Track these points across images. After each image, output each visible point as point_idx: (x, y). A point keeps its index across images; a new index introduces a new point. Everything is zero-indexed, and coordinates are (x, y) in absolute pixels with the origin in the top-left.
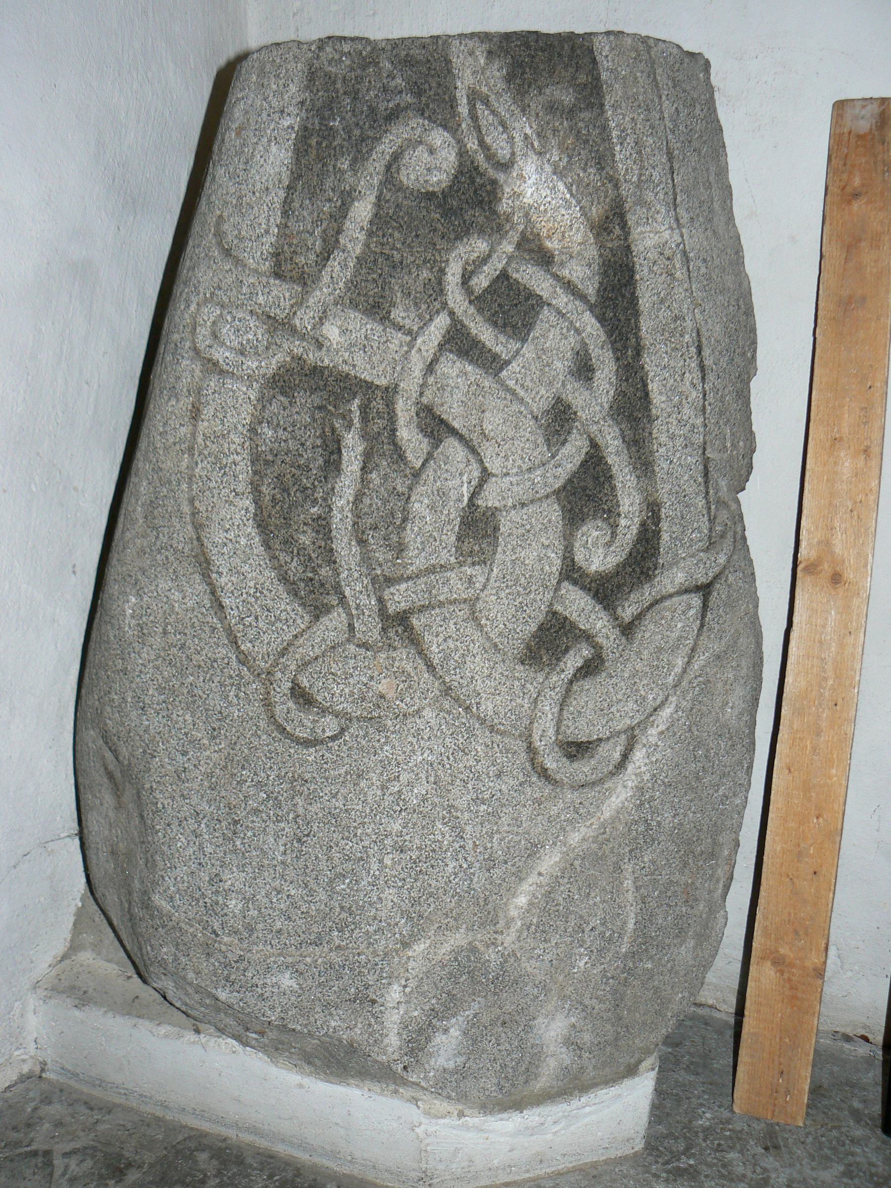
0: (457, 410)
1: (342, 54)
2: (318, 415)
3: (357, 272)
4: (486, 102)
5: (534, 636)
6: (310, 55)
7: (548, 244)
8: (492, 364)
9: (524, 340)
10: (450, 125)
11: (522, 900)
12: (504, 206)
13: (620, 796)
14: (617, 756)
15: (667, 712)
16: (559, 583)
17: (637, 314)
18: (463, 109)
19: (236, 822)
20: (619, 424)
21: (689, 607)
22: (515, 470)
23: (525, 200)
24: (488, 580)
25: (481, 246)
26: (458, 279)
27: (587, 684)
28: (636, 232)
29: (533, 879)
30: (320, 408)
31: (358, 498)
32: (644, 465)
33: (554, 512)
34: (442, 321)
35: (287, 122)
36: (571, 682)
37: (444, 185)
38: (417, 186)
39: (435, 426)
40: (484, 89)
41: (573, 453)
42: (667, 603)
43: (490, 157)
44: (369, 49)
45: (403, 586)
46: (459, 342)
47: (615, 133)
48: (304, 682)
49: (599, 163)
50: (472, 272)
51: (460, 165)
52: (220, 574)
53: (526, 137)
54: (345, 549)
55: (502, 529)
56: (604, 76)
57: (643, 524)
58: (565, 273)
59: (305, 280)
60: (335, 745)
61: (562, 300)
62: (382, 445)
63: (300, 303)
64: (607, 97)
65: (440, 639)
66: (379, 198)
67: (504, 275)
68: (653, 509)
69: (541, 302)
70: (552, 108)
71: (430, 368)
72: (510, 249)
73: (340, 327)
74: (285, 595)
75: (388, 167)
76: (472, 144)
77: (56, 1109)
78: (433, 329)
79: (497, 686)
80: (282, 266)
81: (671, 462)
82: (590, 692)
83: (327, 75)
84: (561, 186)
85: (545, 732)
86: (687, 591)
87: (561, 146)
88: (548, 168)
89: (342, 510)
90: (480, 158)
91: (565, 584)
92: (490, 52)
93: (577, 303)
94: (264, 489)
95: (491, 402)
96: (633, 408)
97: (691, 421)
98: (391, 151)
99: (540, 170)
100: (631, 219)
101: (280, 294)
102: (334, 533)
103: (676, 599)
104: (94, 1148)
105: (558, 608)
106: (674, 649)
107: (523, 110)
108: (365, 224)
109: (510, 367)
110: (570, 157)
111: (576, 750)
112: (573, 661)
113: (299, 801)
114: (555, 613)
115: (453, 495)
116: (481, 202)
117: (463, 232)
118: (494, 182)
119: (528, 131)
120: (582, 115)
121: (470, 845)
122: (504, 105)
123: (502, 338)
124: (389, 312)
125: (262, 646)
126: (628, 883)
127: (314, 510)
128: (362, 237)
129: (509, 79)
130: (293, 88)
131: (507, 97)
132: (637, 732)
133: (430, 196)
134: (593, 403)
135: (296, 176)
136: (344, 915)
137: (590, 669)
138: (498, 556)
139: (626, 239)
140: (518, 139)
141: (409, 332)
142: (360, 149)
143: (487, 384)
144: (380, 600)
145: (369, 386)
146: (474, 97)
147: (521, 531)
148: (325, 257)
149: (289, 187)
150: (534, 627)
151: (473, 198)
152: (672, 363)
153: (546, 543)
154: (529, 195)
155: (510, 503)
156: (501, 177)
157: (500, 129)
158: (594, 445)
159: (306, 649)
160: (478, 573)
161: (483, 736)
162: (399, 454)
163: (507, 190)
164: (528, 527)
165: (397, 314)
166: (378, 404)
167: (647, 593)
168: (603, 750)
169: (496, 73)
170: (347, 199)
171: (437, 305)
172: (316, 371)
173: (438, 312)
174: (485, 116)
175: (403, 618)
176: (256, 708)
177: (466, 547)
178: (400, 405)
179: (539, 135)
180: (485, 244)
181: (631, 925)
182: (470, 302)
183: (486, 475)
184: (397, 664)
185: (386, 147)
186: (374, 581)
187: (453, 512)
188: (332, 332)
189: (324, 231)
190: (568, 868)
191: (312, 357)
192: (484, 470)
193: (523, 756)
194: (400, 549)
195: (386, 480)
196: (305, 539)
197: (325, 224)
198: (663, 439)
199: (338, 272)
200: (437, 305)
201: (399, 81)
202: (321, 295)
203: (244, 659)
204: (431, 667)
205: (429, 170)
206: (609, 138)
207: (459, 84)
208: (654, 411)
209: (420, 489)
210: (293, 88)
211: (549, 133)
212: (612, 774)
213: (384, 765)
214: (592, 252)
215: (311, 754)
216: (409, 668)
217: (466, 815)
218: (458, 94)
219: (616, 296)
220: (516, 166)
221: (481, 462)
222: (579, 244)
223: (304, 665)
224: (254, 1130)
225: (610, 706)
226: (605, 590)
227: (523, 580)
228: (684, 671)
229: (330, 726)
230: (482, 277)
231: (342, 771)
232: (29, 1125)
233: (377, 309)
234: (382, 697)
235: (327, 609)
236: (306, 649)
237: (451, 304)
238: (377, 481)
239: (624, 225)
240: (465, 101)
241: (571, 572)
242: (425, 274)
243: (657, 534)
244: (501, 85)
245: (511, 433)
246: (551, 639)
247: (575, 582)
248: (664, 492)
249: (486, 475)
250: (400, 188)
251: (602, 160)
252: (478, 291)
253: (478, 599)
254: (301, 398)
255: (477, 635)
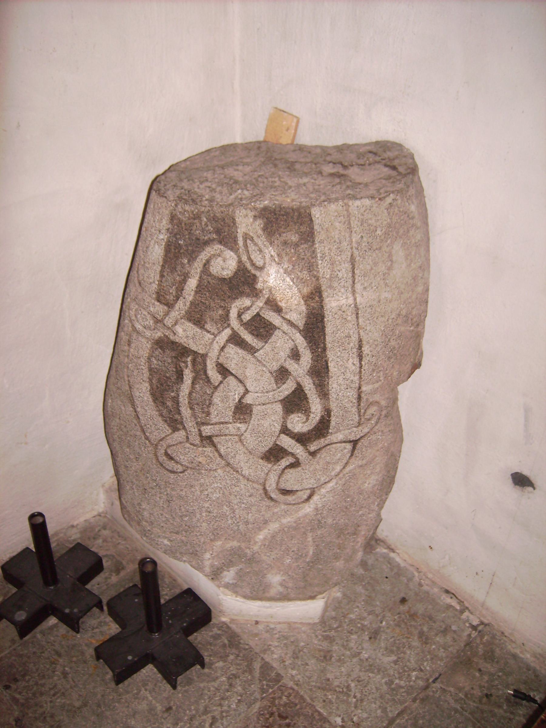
0: (233, 366)
1: (185, 211)
2: (174, 360)
3: (190, 308)
4: (252, 239)
5: (267, 451)
6: (172, 208)
7: (280, 304)
8: (252, 350)
9: (266, 342)
10: (234, 248)
11: (261, 537)
12: (259, 286)
13: (308, 509)
14: (305, 497)
15: (331, 485)
16: (279, 434)
17: (324, 335)
18: (241, 242)
19: (145, 489)
20: (312, 378)
21: (345, 448)
22: (260, 392)
23: (269, 284)
24: (247, 429)
25: (247, 302)
26: (236, 315)
27: (291, 471)
28: (326, 300)
29: (266, 531)
30: (175, 357)
31: (190, 393)
32: (324, 394)
33: (279, 408)
34: (227, 332)
35: (161, 237)
36: (284, 469)
37: (230, 276)
38: (217, 275)
39: (224, 371)
40: (251, 234)
41: (288, 388)
42: (334, 446)
43: (253, 264)
44: (196, 211)
45: (209, 427)
46: (236, 340)
47: (319, 255)
48: (169, 452)
49: (309, 269)
50: (243, 313)
51: (239, 266)
52: (138, 407)
53: (272, 256)
54: (186, 412)
55: (254, 412)
56: (316, 227)
57: (322, 416)
58: (288, 317)
59: (170, 306)
60: (181, 475)
61: (286, 327)
62: (200, 374)
63: (167, 314)
64: (317, 238)
65: (225, 447)
66: (200, 277)
67: (258, 315)
68: (328, 412)
69: (275, 328)
70: (285, 243)
71: (223, 349)
72: (261, 305)
73: (183, 329)
74: (161, 421)
75: (205, 265)
76: (244, 258)
77: (106, 533)
78: (223, 334)
79: (252, 467)
80: (160, 297)
81: (338, 395)
82: (291, 474)
83: (179, 219)
84: (288, 279)
85: (271, 485)
86: (344, 442)
87: (290, 261)
88: (282, 271)
89: (183, 396)
90: (248, 265)
91: (283, 436)
92: (255, 216)
93: (293, 329)
94: (153, 381)
95: (250, 366)
96: (320, 372)
97: (351, 379)
98: (206, 259)
99: (277, 272)
100: (325, 295)
101: (159, 309)
102: (180, 404)
103: (339, 445)
104: (113, 556)
105: (278, 443)
106: (336, 463)
107: (271, 244)
108: (194, 289)
109: (259, 352)
110: (294, 266)
111: (286, 492)
112: (285, 462)
113: (168, 489)
114: (277, 445)
115: (231, 398)
116: (248, 283)
117: (242, 294)
118: (254, 276)
119: (273, 253)
120: (302, 246)
121: (237, 516)
122: (262, 241)
123: (255, 340)
124: (204, 325)
125: (155, 436)
126: (310, 539)
127: (172, 394)
128: (193, 293)
129: (264, 229)
130: (164, 222)
131: (263, 238)
132: (316, 489)
133: (223, 280)
134: (300, 371)
135: (165, 261)
136: (187, 527)
137: (292, 466)
138: (251, 421)
139: (321, 303)
140: (268, 256)
141: (213, 334)
142: (192, 257)
143: (248, 358)
144: (199, 430)
145: (195, 353)
146: (246, 237)
147: (262, 414)
148: (177, 298)
149: (163, 265)
150: (267, 449)
151: (244, 281)
152: (342, 355)
153: (274, 419)
154: (271, 282)
155: (257, 403)
156: (258, 273)
157: (258, 253)
158: (299, 384)
159: (169, 441)
160: (243, 427)
161: (243, 482)
162: (208, 380)
163: (261, 279)
164: (266, 413)
165: (208, 326)
166: (199, 360)
167: (323, 442)
168: (299, 493)
169: (259, 224)
170: (185, 277)
171: (226, 325)
172: (173, 343)
173: (226, 328)
174: (251, 247)
175: (209, 438)
176: (151, 456)
177: (237, 416)
178: (208, 362)
179: (278, 255)
180: (249, 301)
181: (311, 553)
182: (241, 325)
183: (247, 391)
184: (206, 453)
185: (203, 256)
186: (197, 423)
187: (232, 404)
188: (179, 329)
189: (177, 288)
190: (282, 530)
191: (172, 337)
192: (247, 389)
193: (261, 491)
194: (208, 414)
195: (202, 388)
196: (169, 404)
197: (177, 285)
198: (335, 386)
199: (182, 306)
200: (226, 325)
201: (210, 228)
202: (174, 314)
203: (147, 438)
204: (221, 456)
205: (223, 269)
206: (316, 257)
207: (239, 231)
208: (330, 374)
209: (216, 394)
210: (164, 222)
211: (284, 255)
212: (303, 502)
213: (202, 485)
214: (304, 308)
215: (172, 476)
216: (211, 455)
217: (236, 507)
218: (238, 236)
219: (314, 328)
220: (265, 269)
221: (245, 386)
222: (296, 305)
223: (169, 446)
224: (170, 568)
225: (302, 480)
226: (302, 439)
227: (262, 432)
228: (341, 471)
229: (180, 469)
230: (247, 315)
231: (185, 483)
232: (94, 538)
233: (199, 323)
234: (200, 463)
235: (178, 430)
236: (169, 441)
237: (232, 325)
238: (198, 389)
239: (321, 296)
240: (241, 239)
241: (285, 430)
242: (220, 312)
243: (329, 421)
244: (260, 232)
245: (259, 378)
246: (275, 454)
247: (287, 435)
248: (333, 406)
249: (247, 391)
250: (210, 275)
251: (311, 267)
252: (245, 321)
253: (242, 435)
254: (168, 352)
255: (241, 448)
